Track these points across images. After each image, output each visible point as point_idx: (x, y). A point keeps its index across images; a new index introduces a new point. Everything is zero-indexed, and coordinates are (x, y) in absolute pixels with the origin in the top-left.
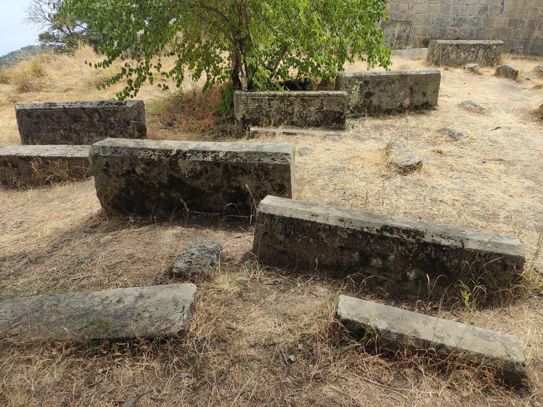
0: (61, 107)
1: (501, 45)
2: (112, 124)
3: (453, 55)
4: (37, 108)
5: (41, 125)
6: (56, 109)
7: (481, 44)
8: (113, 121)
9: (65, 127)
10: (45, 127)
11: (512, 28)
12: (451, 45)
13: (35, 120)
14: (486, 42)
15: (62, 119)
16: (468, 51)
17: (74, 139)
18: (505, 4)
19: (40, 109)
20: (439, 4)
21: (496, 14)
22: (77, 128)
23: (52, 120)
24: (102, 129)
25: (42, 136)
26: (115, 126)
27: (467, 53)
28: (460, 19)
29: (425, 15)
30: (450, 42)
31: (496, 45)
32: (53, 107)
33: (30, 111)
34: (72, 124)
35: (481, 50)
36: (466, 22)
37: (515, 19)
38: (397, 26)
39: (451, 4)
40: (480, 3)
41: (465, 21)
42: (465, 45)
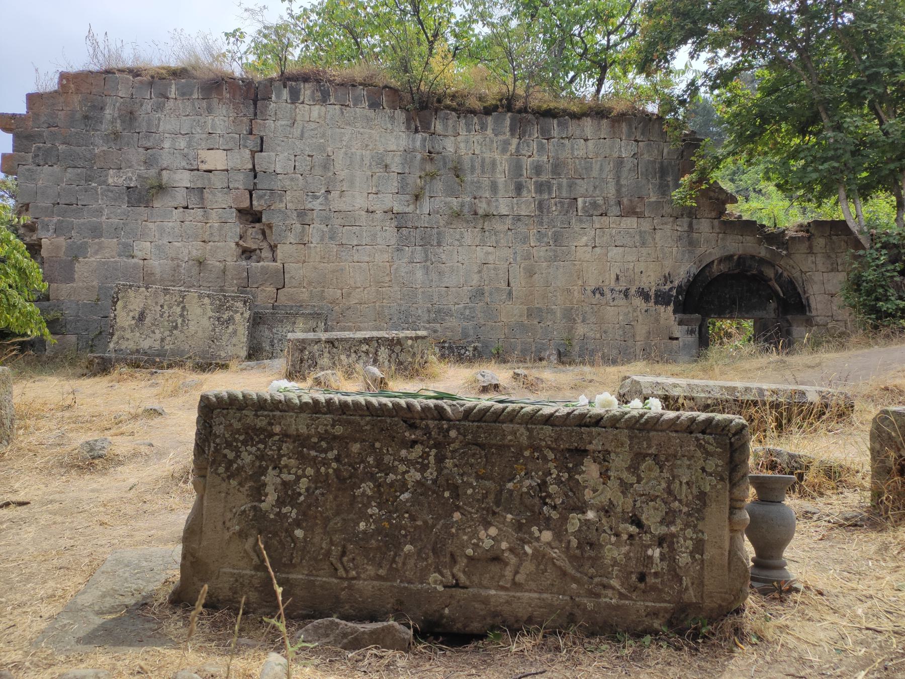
1: (424, 338)
3: (325, 360)
7: (380, 338)
11: (535, 322)
12: (318, 341)
14: (393, 334)
16: (355, 352)
18: (512, 285)
20: (397, 288)
21: (501, 300)
27: (353, 355)
28: (439, 311)
29: (375, 306)
30: (314, 335)
31: (411, 338)
35: (383, 348)
36: (452, 316)
37: (537, 308)
38: (297, 321)
39: (418, 286)
40: (469, 284)
41: (449, 313)
42: (346, 340)
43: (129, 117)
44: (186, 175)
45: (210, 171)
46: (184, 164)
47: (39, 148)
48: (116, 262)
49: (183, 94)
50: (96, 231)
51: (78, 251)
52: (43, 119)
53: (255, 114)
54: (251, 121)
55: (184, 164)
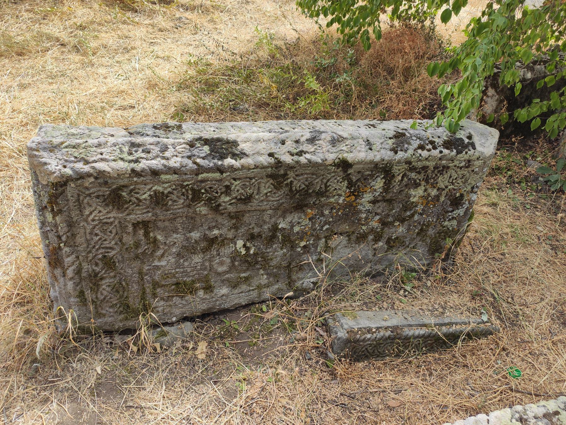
0: (264, 160)
2: (408, 206)
4: (156, 163)
5: (164, 229)
8: (413, 200)
9: (256, 230)
10: (177, 237)
13: (138, 215)
15: (255, 203)
17: (273, 263)
19: (175, 171)
22: (296, 229)
23: (216, 209)
24: (375, 224)
25: (158, 268)
26: (415, 212)
32: (229, 161)
33: (125, 182)
34: (284, 217)
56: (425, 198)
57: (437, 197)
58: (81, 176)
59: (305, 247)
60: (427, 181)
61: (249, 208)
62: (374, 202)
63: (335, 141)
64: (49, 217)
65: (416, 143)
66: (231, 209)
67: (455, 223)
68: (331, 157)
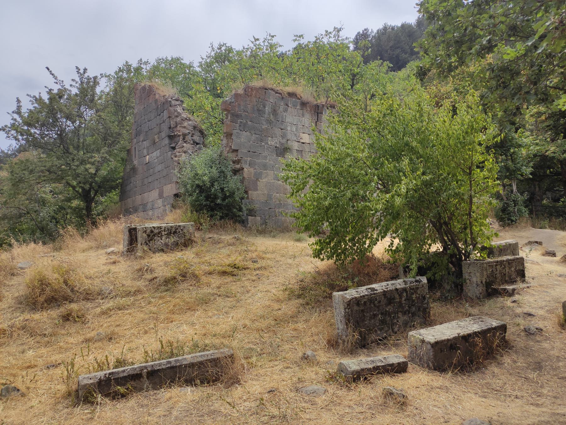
0: (382, 291)
2: (413, 301)
6: (379, 293)
8: (414, 299)
13: (362, 308)
15: (381, 303)
19: (367, 295)
22: (390, 311)
23: (375, 305)
32: (375, 292)
33: (359, 299)
43: (274, 112)
44: (297, 144)
45: (303, 143)
46: (295, 138)
47: (241, 122)
48: (273, 182)
49: (294, 106)
50: (265, 167)
51: (258, 177)
52: (242, 107)
53: (318, 120)
54: (316, 122)
55: (295, 138)
56: (416, 297)
57: (419, 297)
58: (353, 298)
59: (393, 317)
60: (415, 292)
61: (380, 304)
62: (405, 300)
63: (393, 284)
64: (347, 310)
65: (409, 282)
66: (377, 305)
67: (426, 305)
68: (394, 288)
